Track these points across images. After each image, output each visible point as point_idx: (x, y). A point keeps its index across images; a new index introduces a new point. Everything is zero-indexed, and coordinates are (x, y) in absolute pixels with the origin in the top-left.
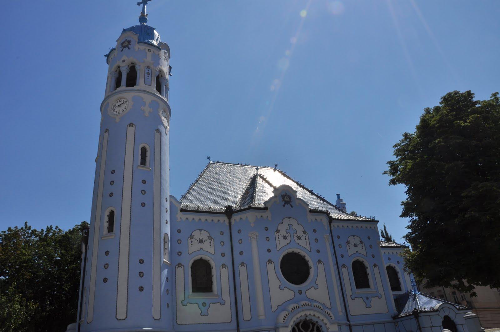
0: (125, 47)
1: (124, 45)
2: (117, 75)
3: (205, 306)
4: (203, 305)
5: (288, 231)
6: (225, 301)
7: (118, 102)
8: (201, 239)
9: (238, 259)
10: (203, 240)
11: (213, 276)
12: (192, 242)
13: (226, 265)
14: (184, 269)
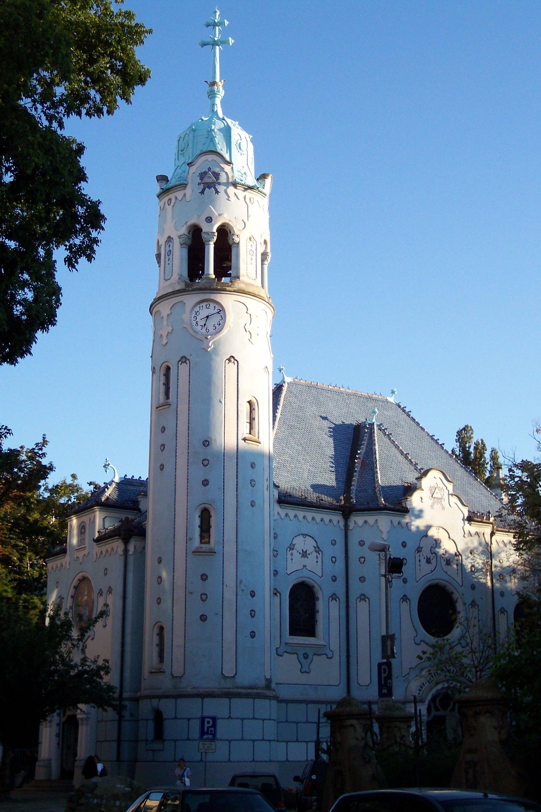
0: (209, 185)
1: (206, 180)
2: (189, 242)
7: (205, 307)
8: (304, 551)
9: (356, 588)
10: (308, 553)
11: (318, 612)
12: (292, 554)
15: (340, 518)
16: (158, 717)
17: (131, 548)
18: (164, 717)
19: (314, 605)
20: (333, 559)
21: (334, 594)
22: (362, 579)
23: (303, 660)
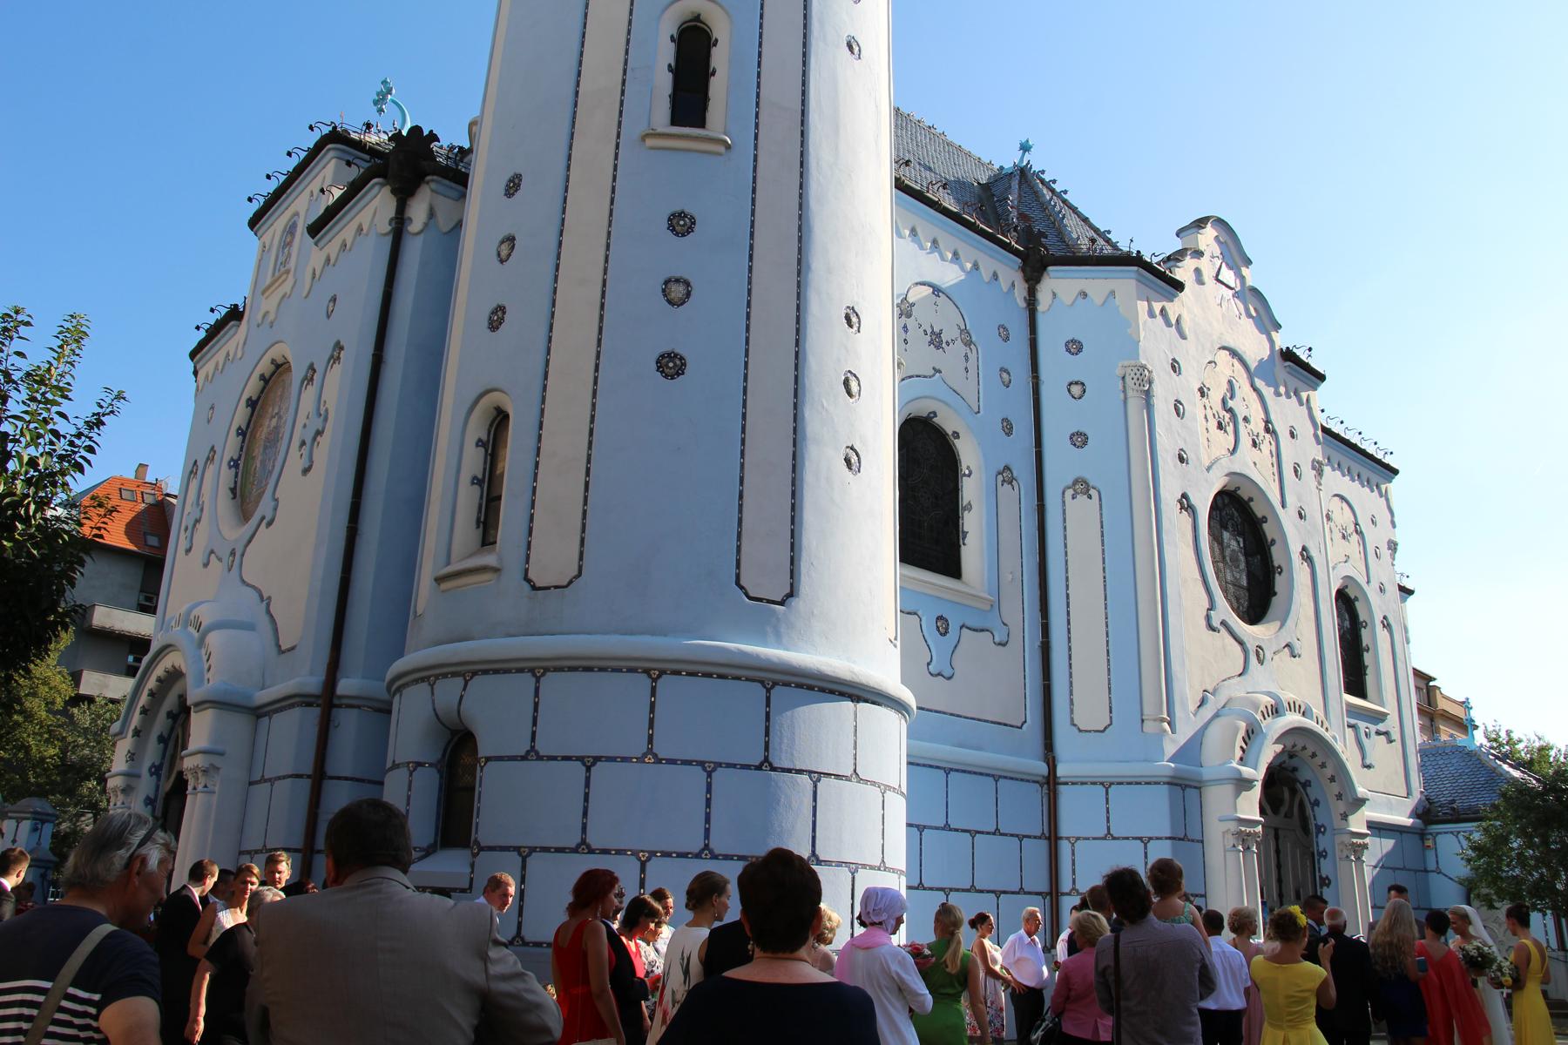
5: (1231, 404)
8: (936, 330)
9: (1061, 464)
15: (1018, 278)
16: (458, 750)
17: (418, 211)
18: (485, 748)
19: (955, 491)
20: (1005, 375)
21: (1007, 468)
22: (1079, 439)
23: (933, 636)
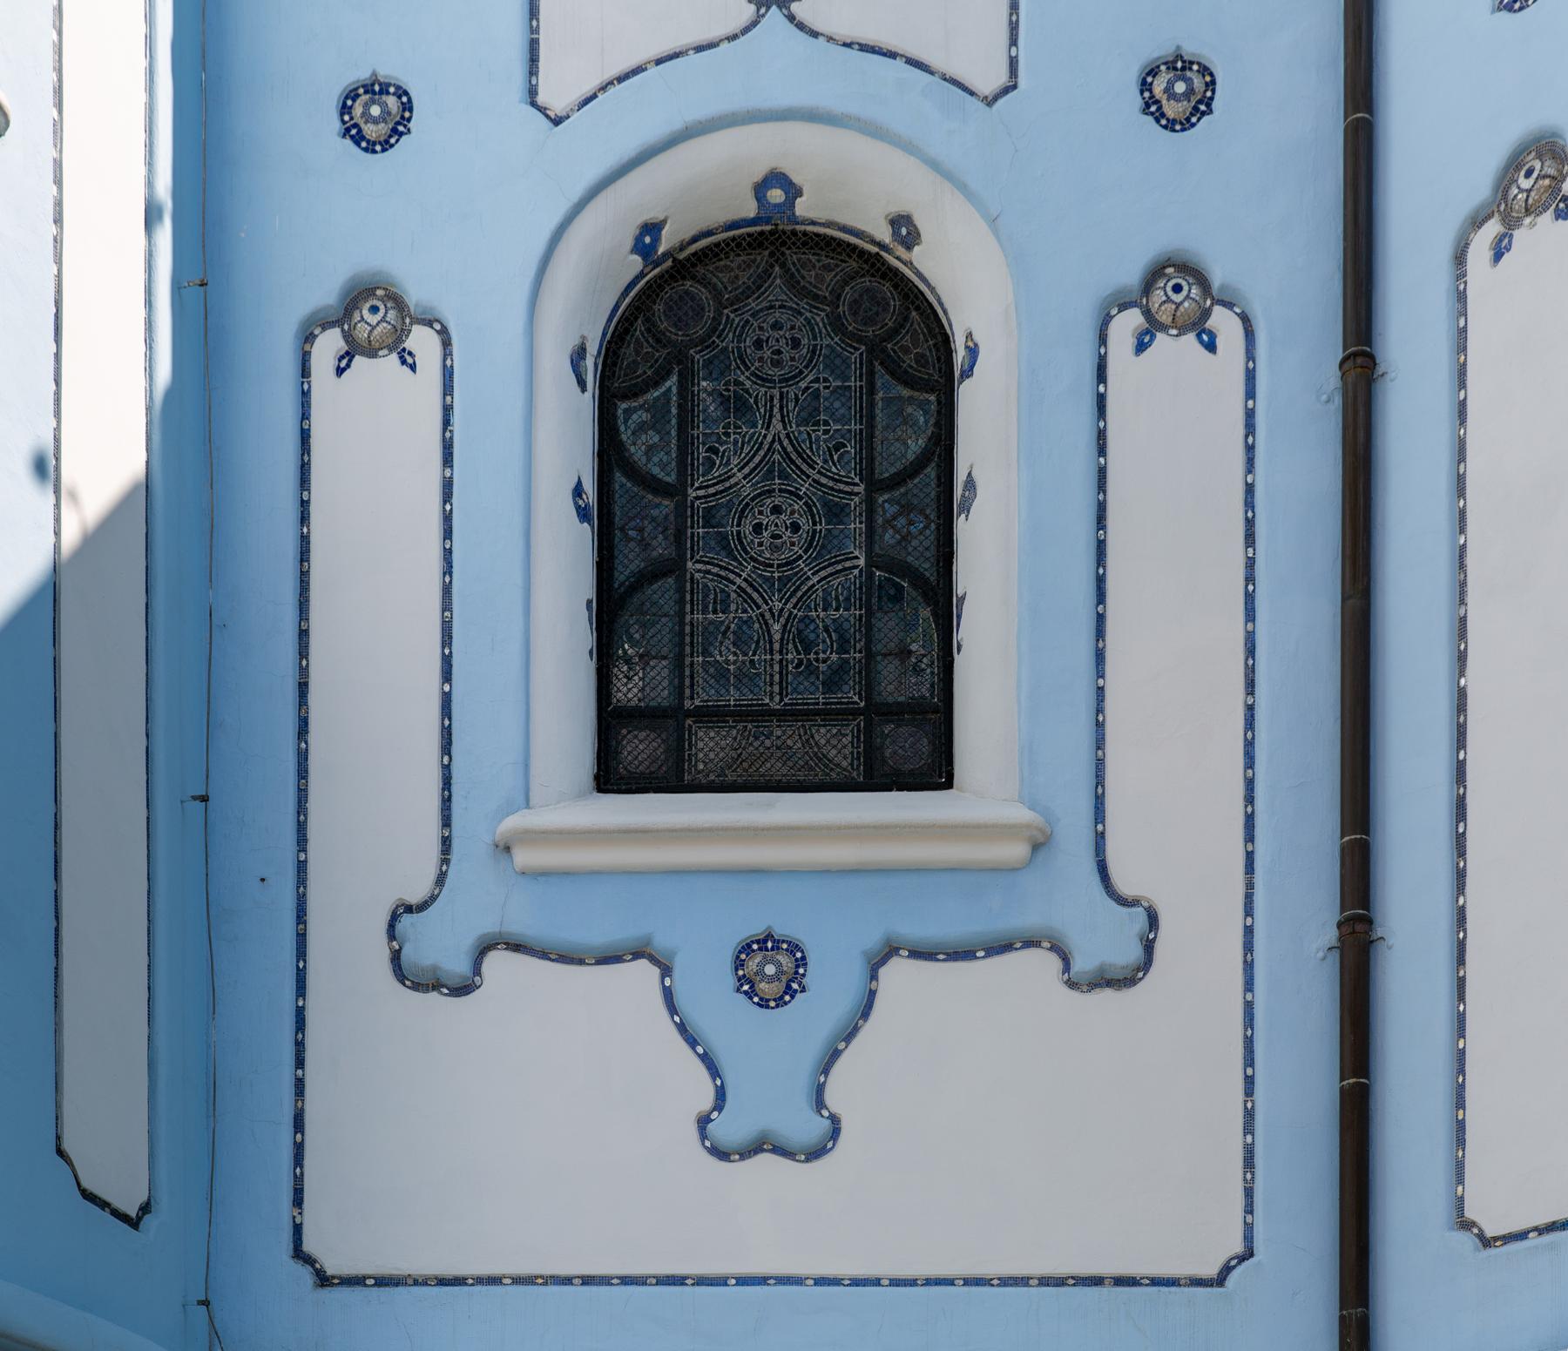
3: (792, 986)
4: (747, 985)
6: (1153, 920)
13: (1216, 281)
14: (448, 388)
